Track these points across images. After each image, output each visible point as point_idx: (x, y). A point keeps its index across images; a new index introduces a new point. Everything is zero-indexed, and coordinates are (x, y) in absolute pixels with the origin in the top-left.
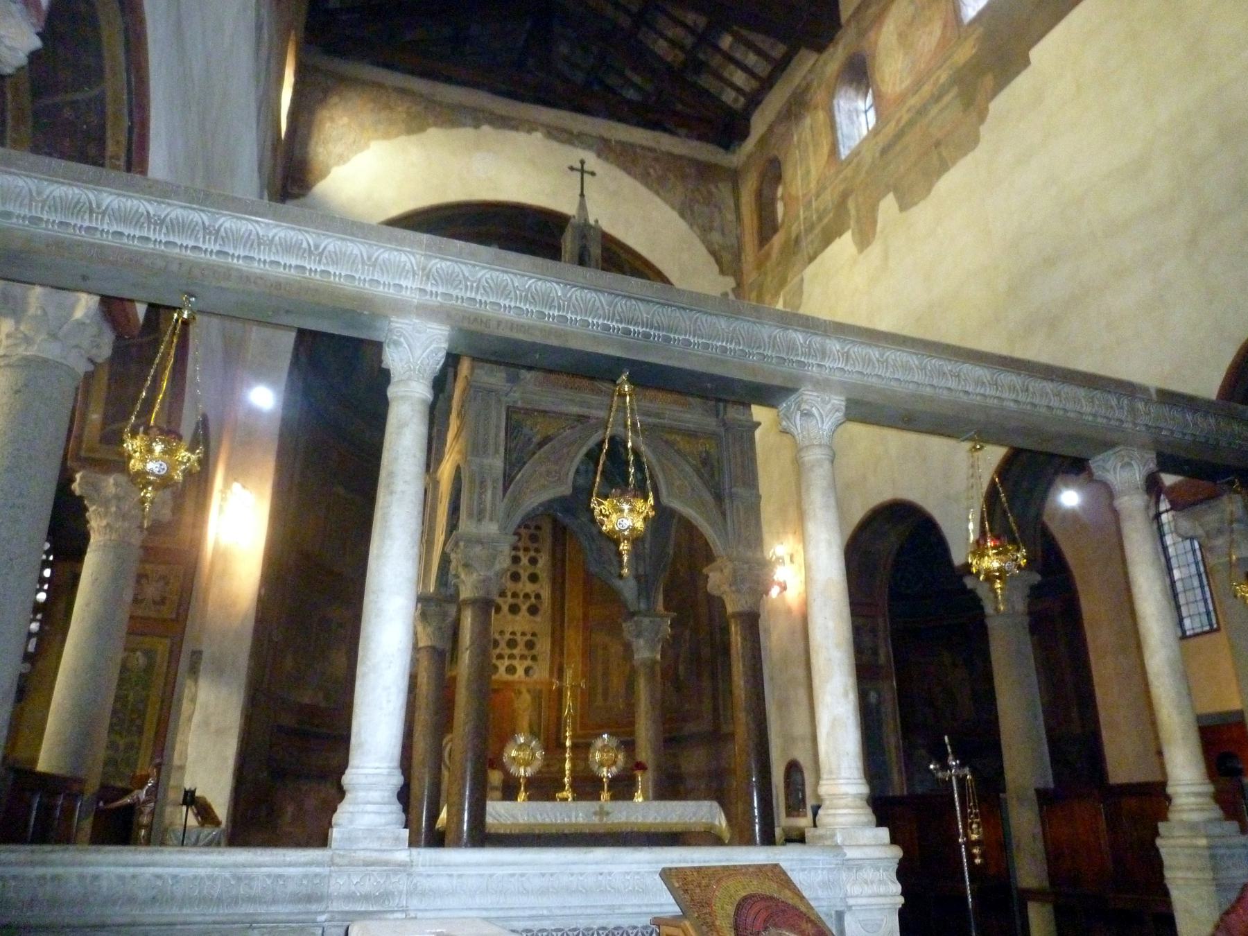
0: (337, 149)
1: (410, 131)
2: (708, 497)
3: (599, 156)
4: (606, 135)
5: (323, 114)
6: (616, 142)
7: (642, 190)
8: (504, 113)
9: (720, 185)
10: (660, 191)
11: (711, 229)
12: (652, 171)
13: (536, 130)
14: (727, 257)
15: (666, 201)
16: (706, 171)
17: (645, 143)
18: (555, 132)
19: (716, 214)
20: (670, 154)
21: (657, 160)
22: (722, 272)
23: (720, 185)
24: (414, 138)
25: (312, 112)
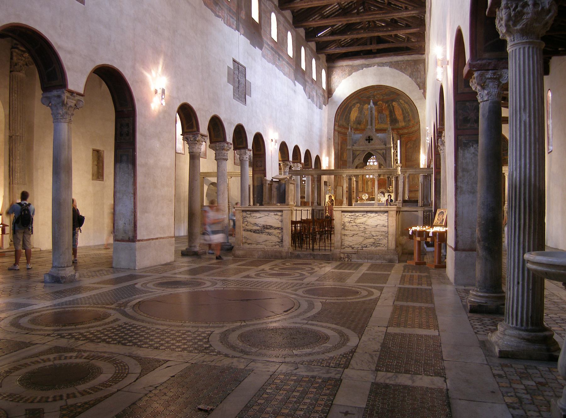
0: (336, 84)
1: (349, 75)
2: (383, 159)
3: (390, 67)
4: (391, 60)
5: (333, 77)
6: (394, 62)
7: (400, 73)
8: (368, 63)
9: (420, 65)
10: (405, 72)
11: (418, 78)
12: (403, 67)
13: (375, 65)
14: (421, 85)
15: (406, 74)
16: (416, 62)
17: (401, 60)
18: (380, 64)
19: (419, 74)
20: (408, 60)
21: (403, 63)
22: (420, 89)
23: (420, 65)
24: (350, 76)
25: (331, 77)
